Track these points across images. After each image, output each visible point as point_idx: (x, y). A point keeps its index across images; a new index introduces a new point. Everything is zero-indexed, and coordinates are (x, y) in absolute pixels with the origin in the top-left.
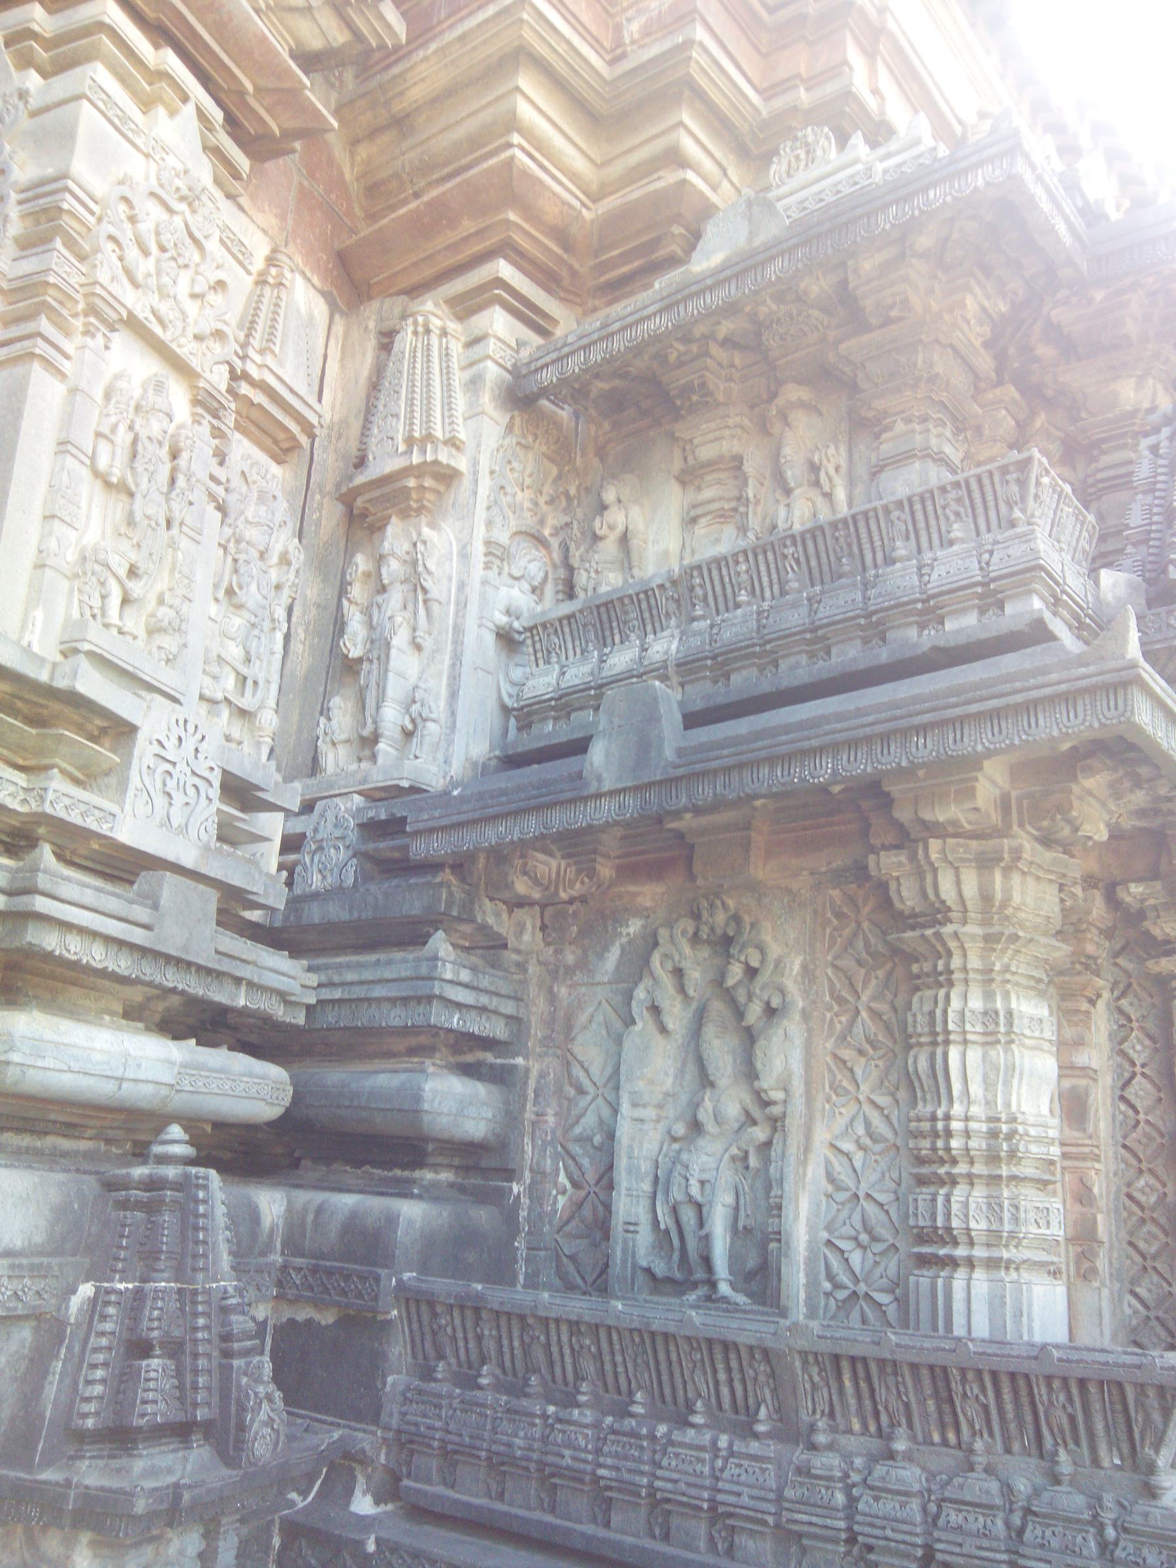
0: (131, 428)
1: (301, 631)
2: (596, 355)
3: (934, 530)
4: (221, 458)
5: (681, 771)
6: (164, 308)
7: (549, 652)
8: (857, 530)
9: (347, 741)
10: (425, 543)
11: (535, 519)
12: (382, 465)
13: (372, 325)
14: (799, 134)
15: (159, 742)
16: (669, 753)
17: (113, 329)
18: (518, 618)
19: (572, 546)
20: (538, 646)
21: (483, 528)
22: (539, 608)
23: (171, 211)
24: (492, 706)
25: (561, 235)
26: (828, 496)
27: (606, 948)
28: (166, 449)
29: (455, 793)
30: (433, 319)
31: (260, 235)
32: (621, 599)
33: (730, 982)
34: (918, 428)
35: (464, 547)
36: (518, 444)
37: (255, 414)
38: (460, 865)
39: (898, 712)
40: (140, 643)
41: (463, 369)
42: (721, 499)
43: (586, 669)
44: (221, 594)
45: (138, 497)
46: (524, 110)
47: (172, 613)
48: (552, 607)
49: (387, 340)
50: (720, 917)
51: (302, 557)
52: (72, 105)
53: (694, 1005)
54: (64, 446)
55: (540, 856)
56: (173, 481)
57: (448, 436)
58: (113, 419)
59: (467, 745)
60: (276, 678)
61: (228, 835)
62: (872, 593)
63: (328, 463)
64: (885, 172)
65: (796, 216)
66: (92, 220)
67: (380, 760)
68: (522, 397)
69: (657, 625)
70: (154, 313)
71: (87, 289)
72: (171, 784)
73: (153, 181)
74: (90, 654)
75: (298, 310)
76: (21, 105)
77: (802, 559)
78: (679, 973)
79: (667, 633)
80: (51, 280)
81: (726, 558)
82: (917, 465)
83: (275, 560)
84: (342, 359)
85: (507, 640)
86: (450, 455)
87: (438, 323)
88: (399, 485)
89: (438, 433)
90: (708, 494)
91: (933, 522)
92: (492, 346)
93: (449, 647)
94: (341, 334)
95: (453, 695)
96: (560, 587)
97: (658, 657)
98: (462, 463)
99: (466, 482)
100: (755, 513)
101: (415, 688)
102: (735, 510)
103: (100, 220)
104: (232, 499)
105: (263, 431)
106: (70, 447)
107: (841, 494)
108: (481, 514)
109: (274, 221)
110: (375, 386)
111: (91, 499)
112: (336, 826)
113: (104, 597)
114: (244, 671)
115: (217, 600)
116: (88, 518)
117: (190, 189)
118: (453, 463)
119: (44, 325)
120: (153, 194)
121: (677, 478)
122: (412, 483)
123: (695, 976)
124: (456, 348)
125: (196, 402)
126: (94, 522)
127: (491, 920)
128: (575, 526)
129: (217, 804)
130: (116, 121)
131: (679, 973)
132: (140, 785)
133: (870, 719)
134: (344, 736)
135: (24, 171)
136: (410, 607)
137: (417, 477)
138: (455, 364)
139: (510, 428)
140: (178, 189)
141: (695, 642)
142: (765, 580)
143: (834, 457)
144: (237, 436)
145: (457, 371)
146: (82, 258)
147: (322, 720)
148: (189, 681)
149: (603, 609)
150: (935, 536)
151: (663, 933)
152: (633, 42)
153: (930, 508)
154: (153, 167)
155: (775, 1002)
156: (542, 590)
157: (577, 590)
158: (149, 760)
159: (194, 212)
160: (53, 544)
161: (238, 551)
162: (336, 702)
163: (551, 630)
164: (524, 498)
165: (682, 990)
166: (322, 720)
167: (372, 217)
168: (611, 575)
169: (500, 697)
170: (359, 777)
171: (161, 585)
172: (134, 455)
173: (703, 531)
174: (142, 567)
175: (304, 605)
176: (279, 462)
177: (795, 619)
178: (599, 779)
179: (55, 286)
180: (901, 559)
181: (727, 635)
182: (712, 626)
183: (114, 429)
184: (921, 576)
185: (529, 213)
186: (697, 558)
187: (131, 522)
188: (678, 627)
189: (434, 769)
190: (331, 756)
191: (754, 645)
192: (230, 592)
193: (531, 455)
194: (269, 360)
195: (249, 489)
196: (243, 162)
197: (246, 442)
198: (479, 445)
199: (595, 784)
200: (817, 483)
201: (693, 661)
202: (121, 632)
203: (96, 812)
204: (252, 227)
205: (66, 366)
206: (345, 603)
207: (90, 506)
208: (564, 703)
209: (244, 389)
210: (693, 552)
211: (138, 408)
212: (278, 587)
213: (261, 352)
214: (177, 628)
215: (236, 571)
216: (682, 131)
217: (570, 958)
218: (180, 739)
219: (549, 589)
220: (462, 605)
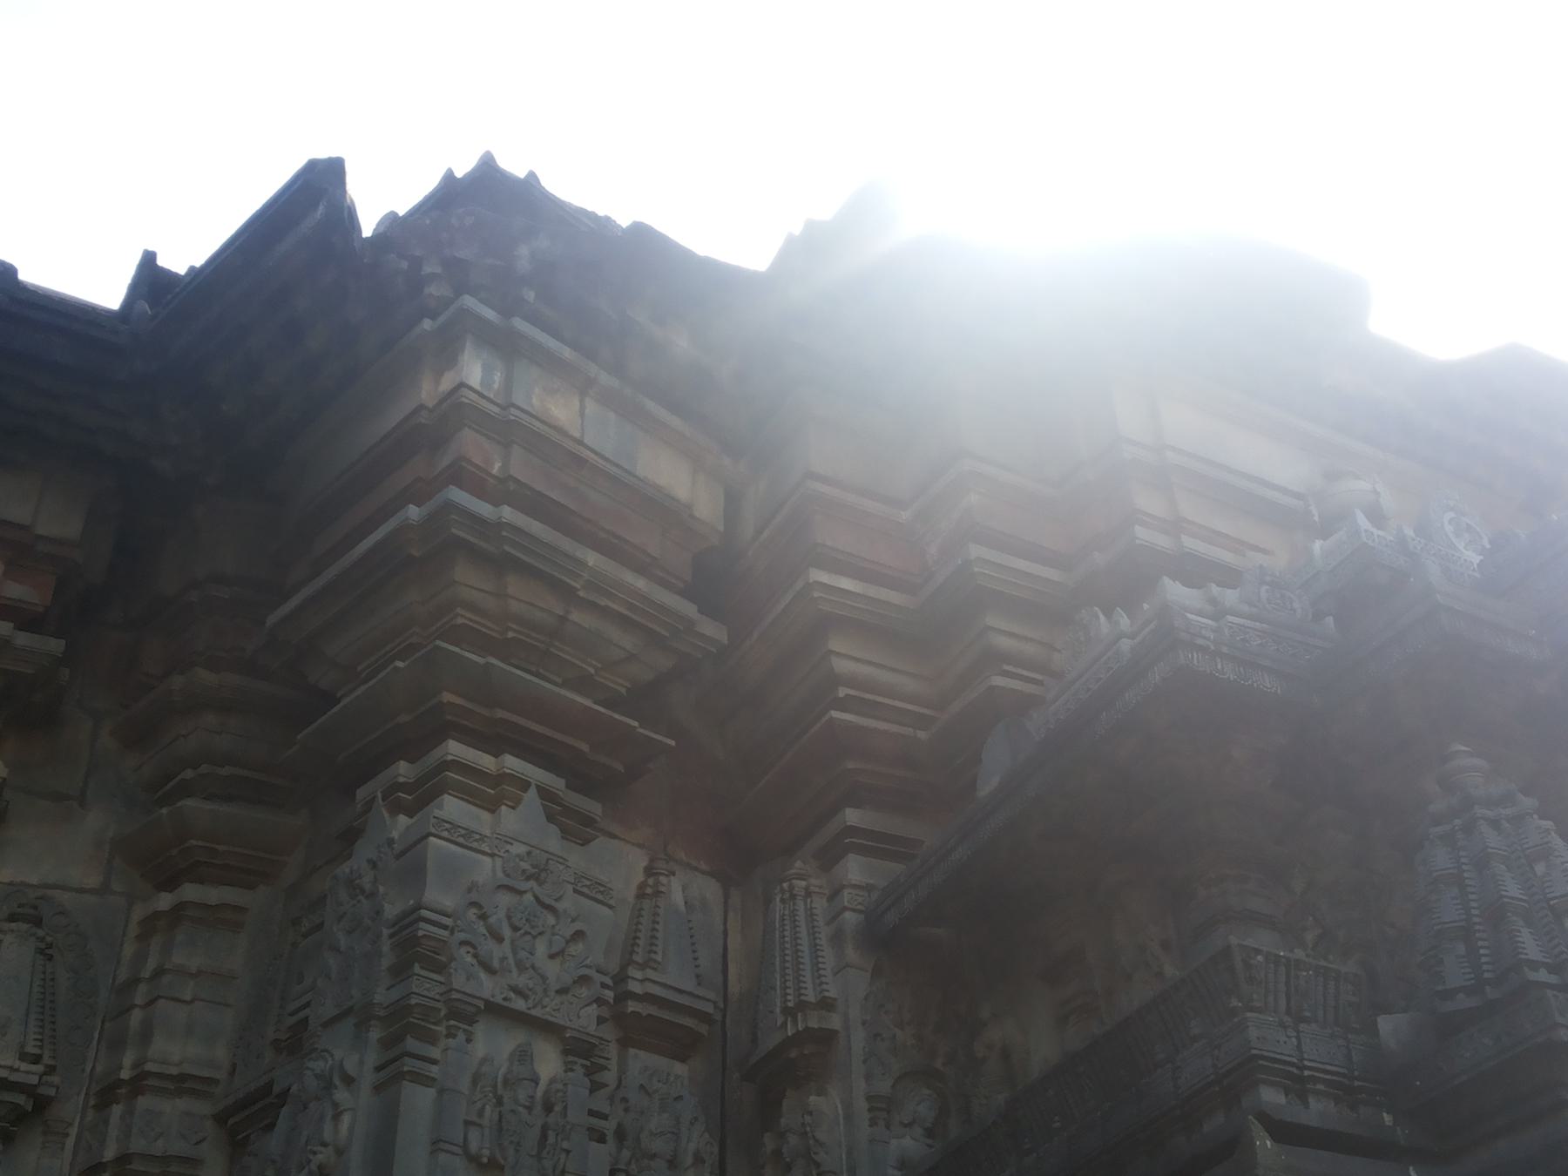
6: (521, 981)
10: (810, 1113)
17: (472, 1022)
41: (828, 924)
46: (842, 666)
54: (437, 1144)
56: (544, 1136)
58: (479, 1105)
66: (445, 933)
73: (500, 874)
80: (413, 1002)
83: (689, 1160)
89: (811, 996)
92: (847, 896)
98: (835, 1022)
103: (452, 933)
106: (442, 1145)
117: (534, 866)
118: (824, 1026)
122: (793, 1054)
124: (820, 904)
125: (566, 1052)
130: (461, 840)
135: (391, 911)
146: (440, 968)
154: (499, 862)
159: (541, 884)
172: (500, 1130)
176: (683, 1061)
183: (481, 1114)
196: (594, 808)
197: (642, 1054)
205: (434, 1070)
209: (632, 1006)
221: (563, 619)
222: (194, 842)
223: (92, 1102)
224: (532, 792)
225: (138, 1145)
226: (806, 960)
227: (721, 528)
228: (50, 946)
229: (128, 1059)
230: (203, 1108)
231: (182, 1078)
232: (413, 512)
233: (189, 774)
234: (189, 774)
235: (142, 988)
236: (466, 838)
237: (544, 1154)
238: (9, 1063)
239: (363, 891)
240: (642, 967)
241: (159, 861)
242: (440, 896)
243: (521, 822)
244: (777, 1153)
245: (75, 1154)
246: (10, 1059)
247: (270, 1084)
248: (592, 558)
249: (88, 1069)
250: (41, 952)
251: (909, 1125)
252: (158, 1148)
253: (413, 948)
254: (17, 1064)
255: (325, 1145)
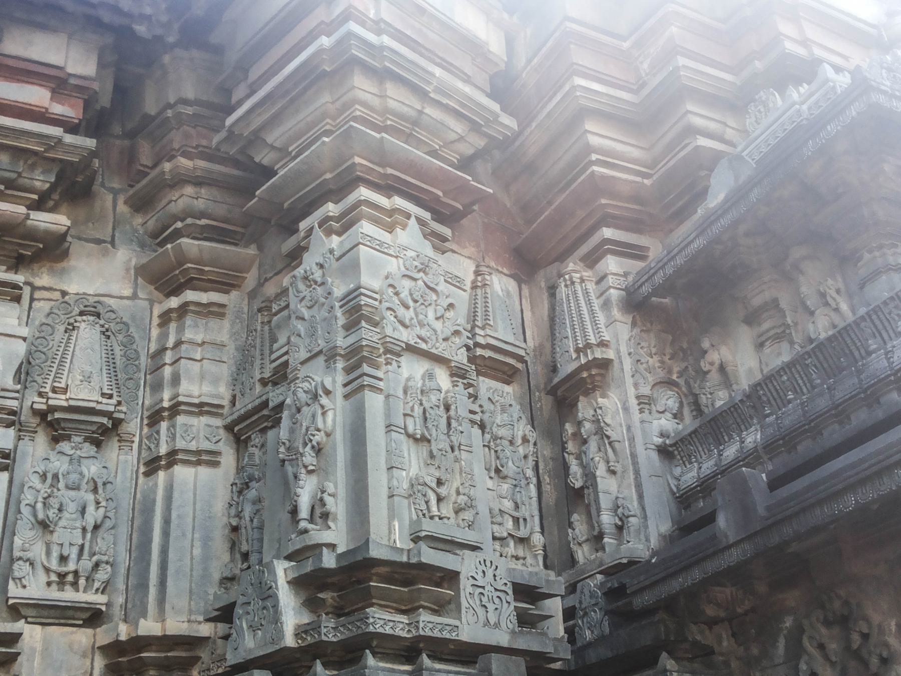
0: (421, 404)
1: (546, 477)
2: (669, 270)
3: (889, 328)
4: (474, 397)
5: (770, 522)
6: (424, 333)
7: (690, 456)
8: (843, 339)
9: (587, 540)
10: (600, 408)
11: (665, 371)
12: (566, 369)
13: (543, 284)
14: (757, 97)
15: (472, 577)
16: (761, 511)
17: (400, 356)
18: (668, 437)
19: (692, 382)
20: (682, 454)
21: (633, 389)
22: (680, 427)
23: (415, 280)
24: (666, 496)
25: (636, 198)
26: (837, 310)
27: (776, 641)
28: (442, 407)
29: (653, 561)
30: (574, 274)
31: (468, 261)
32: (721, 414)
33: (855, 646)
34: (877, 254)
35: (624, 404)
36: (642, 331)
37: (488, 363)
38: (669, 605)
39: (881, 457)
40: (452, 520)
41: (597, 298)
42: (773, 328)
43: (712, 462)
44: (493, 474)
45: (432, 441)
46: (594, 140)
47: (465, 498)
48: (689, 423)
49: (552, 290)
50: (837, 604)
51: (535, 435)
52: (355, 249)
53: (839, 668)
54: (389, 428)
55: (718, 589)
56: (449, 425)
57: (599, 340)
58: (411, 404)
59: (657, 526)
60: (536, 513)
61: (525, 621)
62: (862, 377)
63: (537, 371)
64: (809, 108)
65: (757, 158)
66: (377, 303)
67: (607, 549)
68: (637, 305)
69: (747, 424)
70: (420, 337)
71: (382, 341)
72: (485, 599)
73: (403, 269)
74: (427, 537)
75: (498, 296)
76: (331, 257)
77: (818, 365)
78: (821, 647)
79: (753, 429)
80: (364, 343)
81: (773, 375)
82: (884, 277)
83: (520, 441)
84: (532, 308)
85: (664, 452)
86: (603, 352)
87: (578, 275)
88: (578, 377)
89: (593, 341)
90: (766, 326)
91: (886, 324)
92: (611, 280)
93: (631, 468)
94: (527, 295)
95: (641, 497)
96: (693, 408)
97: (751, 446)
98: (610, 354)
99: (616, 364)
100: (796, 332)
101: (617, 498)
102: (784, 332)
103: (381, 302)
104: (486, 417)
105: (495, 369)
106: (394, 428)
107: (844, 307)
108: (629, 381)
109: (473, 249)
110: (552, 319)
111: (409, 450)
112: (591, 597)
113: (427, 502)
114: (516, 514)
115: (491, 478)
116: (410, 461)
117: (422, 264)
119: (366, 368)
120: (404, 276)
121: (743, 322)
122: (585, 374)
123: (833, 646)
124: (591, 286)
125: (452, 375)
126: (413, 464)
127: (698, 638)
128: (690, 369)
129: (513, 604)
130: (377, 247)
131: (821, 647)
132: (468, 606)
133: (867, 465)
134: (584, 538)
135: (339, 291)
136: (602, 449)
137: (587, 370)
138: (593, 296)
139: (634, 324)
140: (416, 267)
141: (770, 431)
142: (800, 382)
143: (831, 285)
144: (481, 378)
145: (595, 301)
146: (376, 324)
147: (570, 531)
148: (481, 535)
149: (712, 423)
150: (891, 332)
151: (805, 622)
152: (647, 75)
153: (882, 316)
154: (401, 261)
155: (885, 654)
156: (682, 415)
157: (703, 407)
158: (470, 589)
160: (395, 483)
161: (497, 446)
162: (575, 517)
163: (687, 443)
164: (654, 361)
165: (827, 658)
166: (570, 531)
167: (529, 222)
168: (720, 393)
169: (671, 490)
170: (597, 562)
171: (456, 484)
172: (426, 419)
173: (769, 350)
174: (443, 478)
175: (544, 461)
176: (508, 383)
177: (822, 403)
178: (726, 536)
179: (367, 345)
180: (874, 351)
181: (787, 422)
182: (777, 419)
183: (412, 409)
184: (888, 359)
185: (613, 195)
186: (770, 368)
187: (432, 456)
188: (758, 423)
189: (641, 546)
190: (580, 552)
191: (804, 425)
192: (497, 471)
193: (652, 335)
194: (489, 332)
195: (495, 406)
196: (446, 231)
197: (487, 380)
198: (618, 341)
199: (724, 540)
200: (827, 304)
201: (772, 443)
202: (441, 518)
203: (447, 627)
204: (462, 258)
205: (381, 384)
206: (566, 455)
207: (409, 455)
208: (705, 487)
209: (479, 352)
210: (767, 365)
211: (422, 392)
212: (525, 457)
213: (483, 328)
214: (470, 505)
215: (498, 458)
216: (690, 116)
217: (755, 651)
218: (484, 572)
219: (686, 411)
220: (632, 440)
221: (421, 112)
222: (190, 265)
223: (146, 422)
224: (413, 219)
225: (180, 444)
226: (586, 317)
227: (506, 59)
228: (107, 330)
229: (166, 395)
230: (218, 422)
231: (201, 405)
232: (325, 41)
233: (179, 225)
234: (179, 225)
235: (169, 353)
236: (381, 247)
237: (451, 433)
238: (95, 399)
239: (316, 282)
240: (483, 328)
241: (166, 279)
242: (370, 280)
243: (409, 237)
244: (577, 435)
245: (140, 453)
246: (97, 397)
247: (267, 401)
248: (438, 72)
249: (140, 403)
250: (103, 333)
251: (662, 412)
252: (193, 446)
253: (356, 313)
254: (100, 399)
255: (319, 430)
